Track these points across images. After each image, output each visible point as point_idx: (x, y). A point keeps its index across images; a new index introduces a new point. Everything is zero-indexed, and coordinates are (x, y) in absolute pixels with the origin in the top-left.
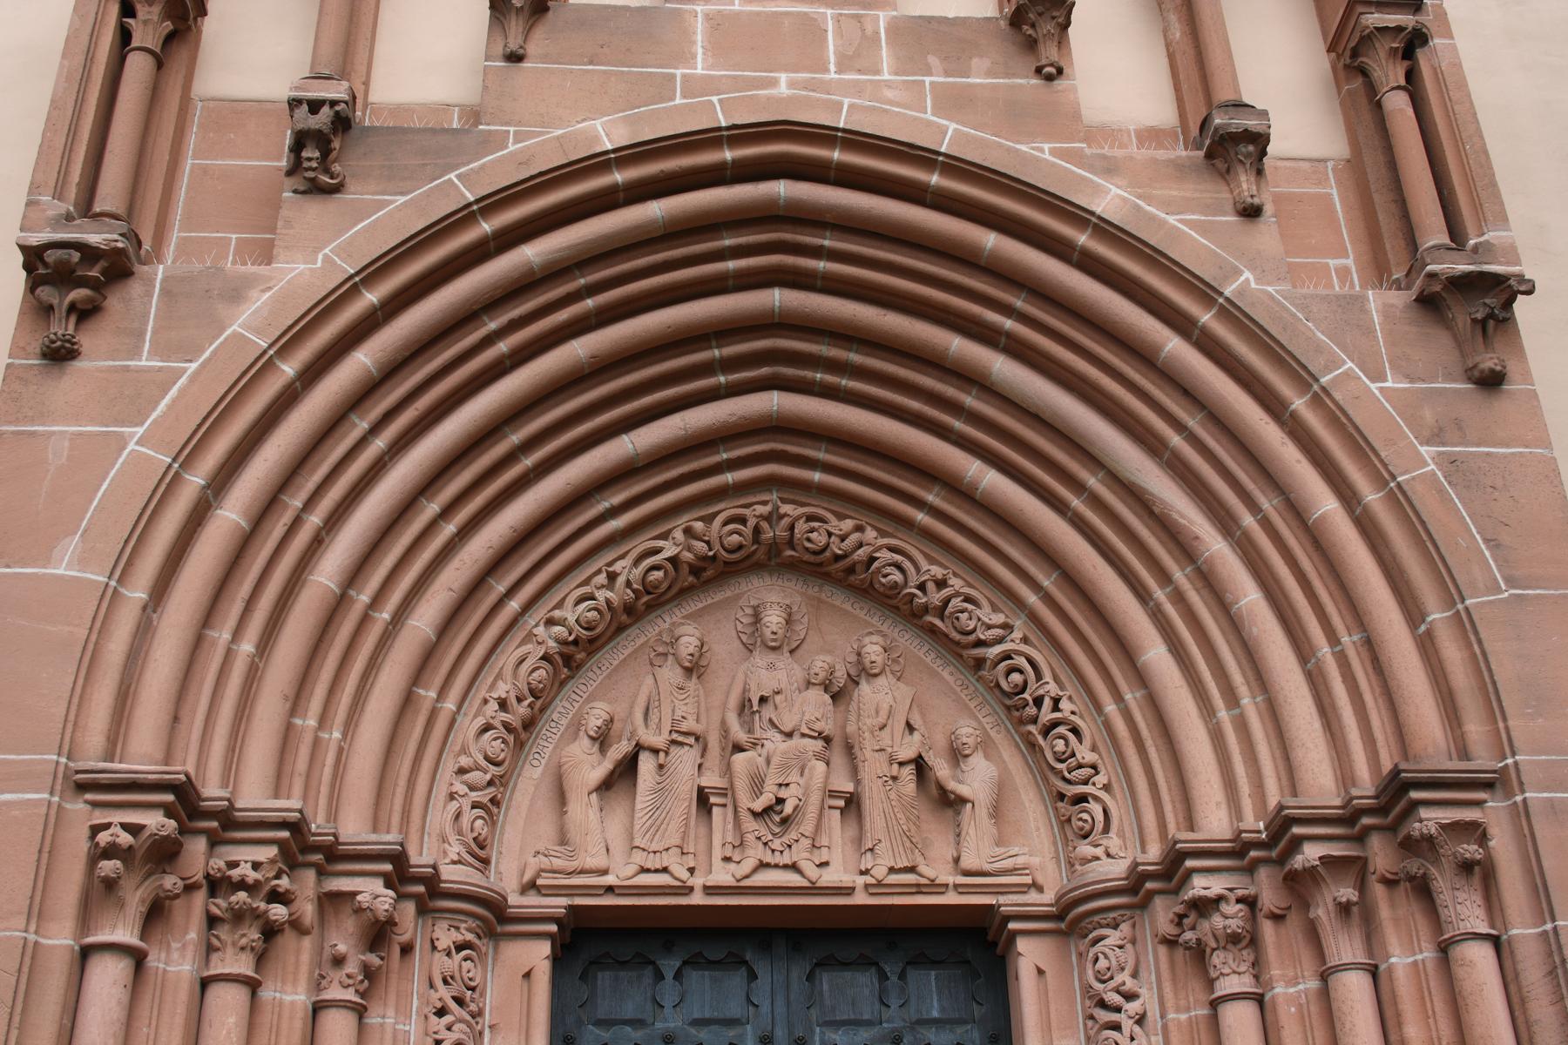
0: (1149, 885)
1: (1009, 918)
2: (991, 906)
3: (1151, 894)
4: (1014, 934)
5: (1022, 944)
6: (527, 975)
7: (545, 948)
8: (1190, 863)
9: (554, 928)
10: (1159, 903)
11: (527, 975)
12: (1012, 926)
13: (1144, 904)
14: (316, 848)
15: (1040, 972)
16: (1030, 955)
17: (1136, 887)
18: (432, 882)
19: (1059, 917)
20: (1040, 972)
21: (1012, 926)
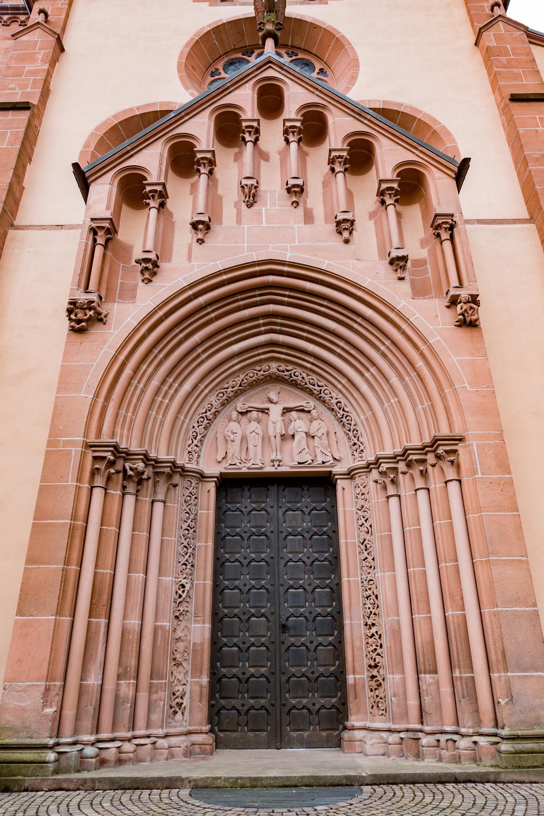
0: (371, 466)
1: (335, 475)
2: (331, 471)
3: (372, 468)
4: (337, 479)
5: (339, 482)
6: (209, 491)
7: (214, 484)
8: (381, 461)
9: (216, 479)
10: (373, 470)
11: (209, 491)
12: (336, 477)
13: (370, 471)
14: (152, 460)
15: (344, 489)
16: (340, 484)
17: (368, 467)
18: (183, 468)
19: (349, 474)
20: (344, 489)
21: (336, 477)
